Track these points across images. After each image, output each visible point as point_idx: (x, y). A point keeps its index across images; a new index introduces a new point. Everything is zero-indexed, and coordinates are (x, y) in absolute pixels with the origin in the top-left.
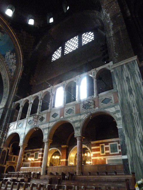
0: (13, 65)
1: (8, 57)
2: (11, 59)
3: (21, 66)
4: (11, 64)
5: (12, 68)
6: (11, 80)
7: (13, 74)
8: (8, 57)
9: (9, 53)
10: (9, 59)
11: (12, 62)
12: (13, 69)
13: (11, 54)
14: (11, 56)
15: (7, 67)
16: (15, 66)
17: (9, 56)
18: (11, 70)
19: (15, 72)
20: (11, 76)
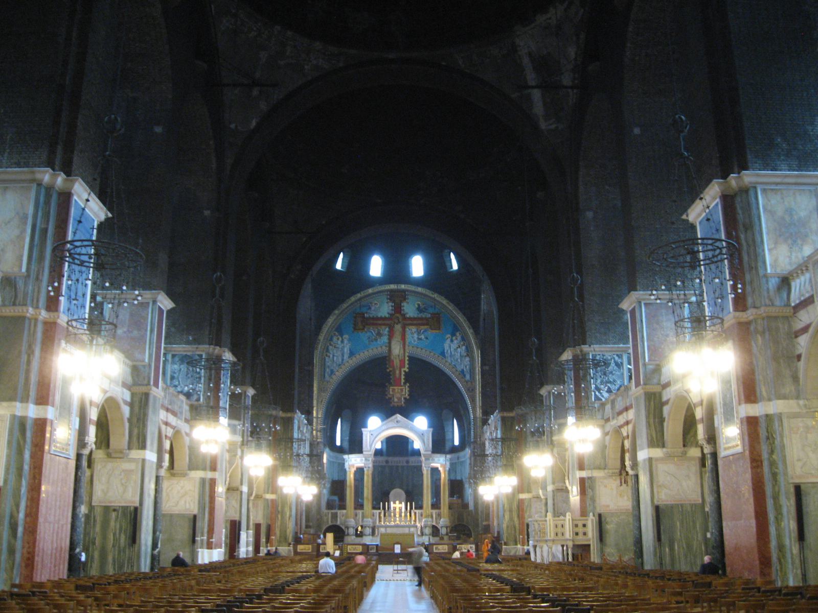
0: (463, 359)
1: (449, 351)
2: (456, 350)
3: (477, 354)
4: (459, 360)
5: (462, 367)
6: (469, 390)
7: (468, 377)
8: (449, 351)
9: (449, 340)
10: (453, 353)
11: (459, 355)
12: (466, 367)
13: (452, 341)
14: (454, 345)
15: (454, 370)
16: (468, 359)
17: (450, 347)
18: (463, 371)
19: (470, 370)
20: (467, 382)
